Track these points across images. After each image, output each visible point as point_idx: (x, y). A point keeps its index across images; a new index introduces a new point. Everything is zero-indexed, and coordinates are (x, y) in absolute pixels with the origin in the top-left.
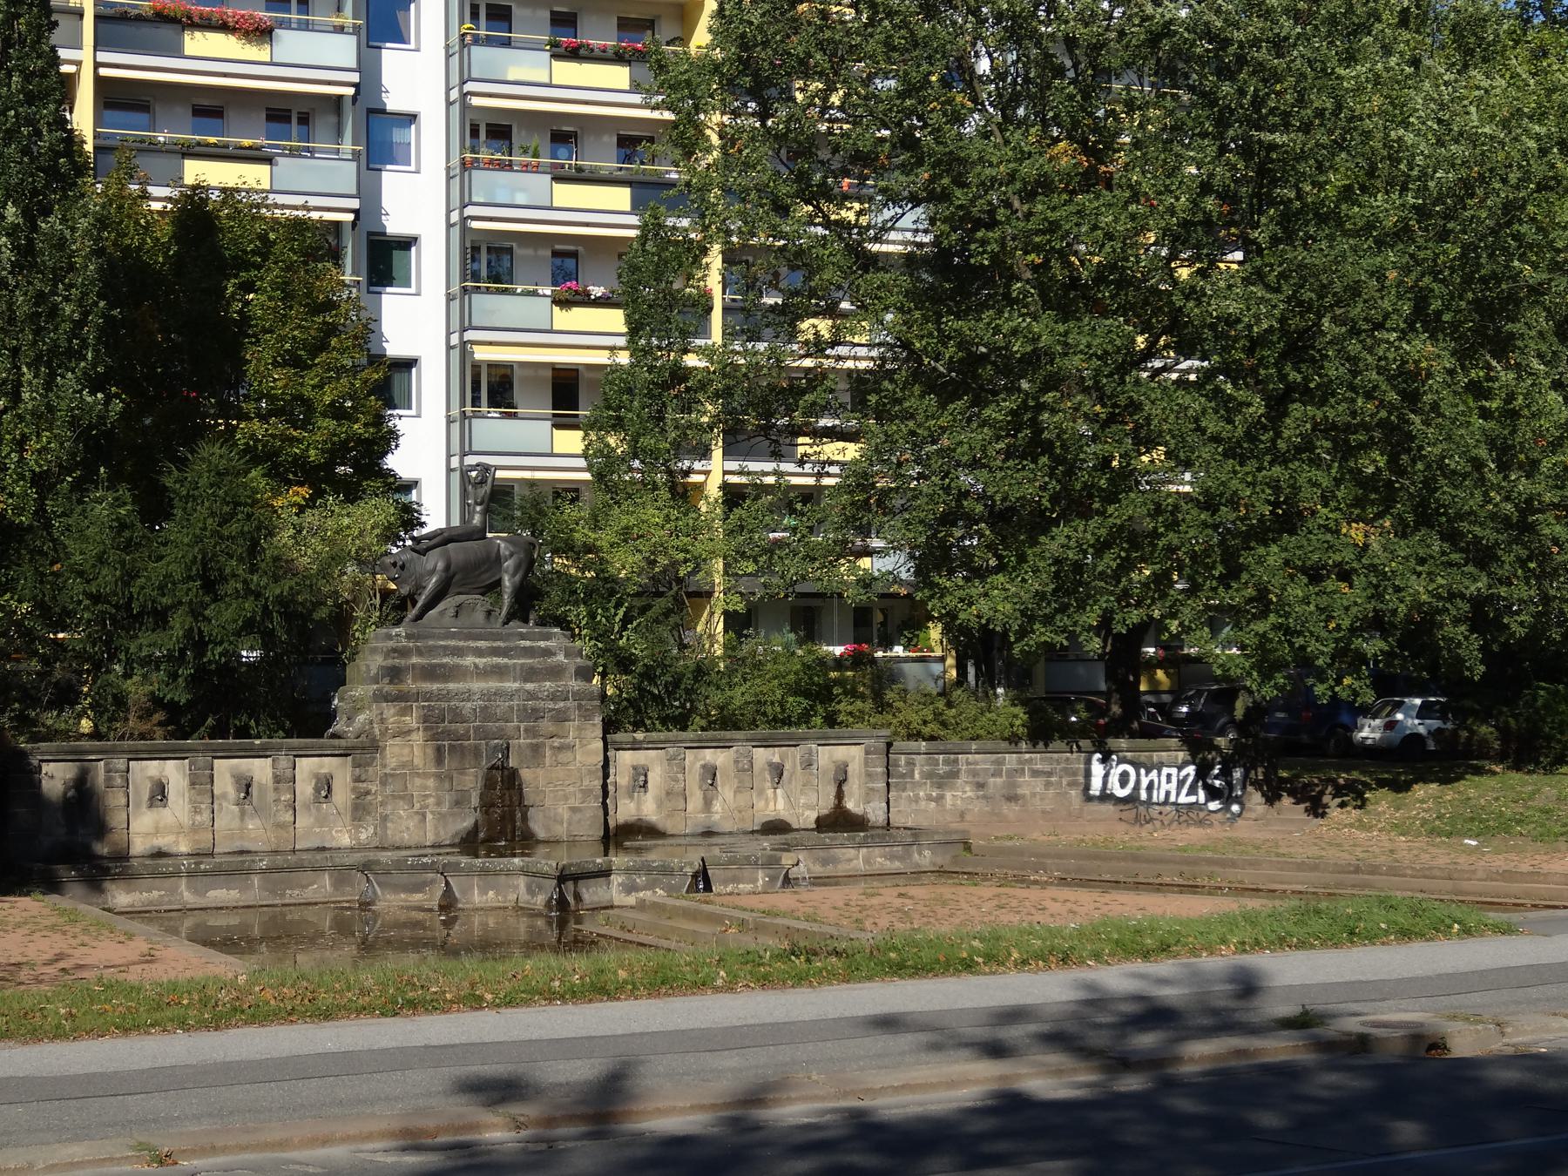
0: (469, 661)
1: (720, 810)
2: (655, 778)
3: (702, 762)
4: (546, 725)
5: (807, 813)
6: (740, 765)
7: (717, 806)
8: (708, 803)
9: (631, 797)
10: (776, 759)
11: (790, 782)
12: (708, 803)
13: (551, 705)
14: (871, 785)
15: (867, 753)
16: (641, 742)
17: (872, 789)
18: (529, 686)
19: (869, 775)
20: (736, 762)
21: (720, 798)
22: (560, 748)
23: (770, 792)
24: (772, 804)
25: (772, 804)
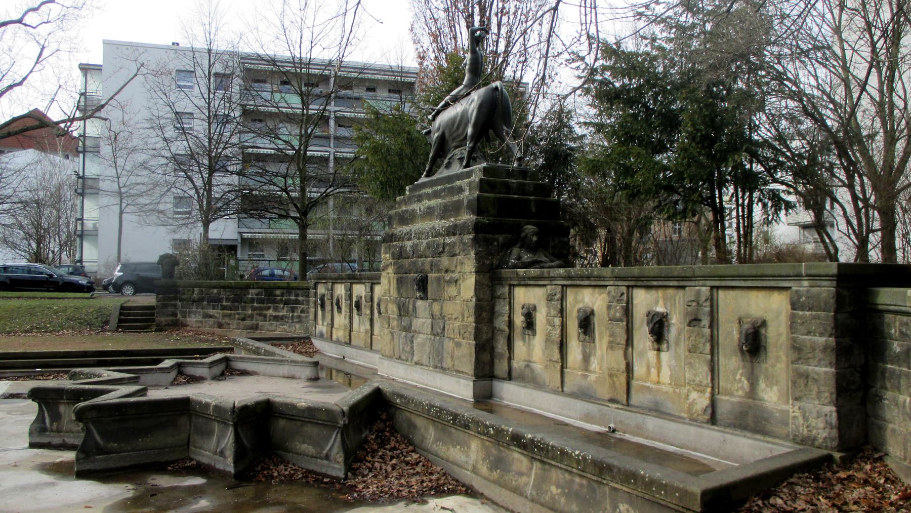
0: (416, 207)
1: (597, 370)
2: (540, 318)
3: (581, 305)
4: (445, 261)
5: (694, 395)
6: (612, 312)
7: (594, 365)
8: (586, 359)
9: (524, 339)
10: (660, 309)
11: (677, 343)
12: (586, 359)
13: (448, 240)
14: (803, 367)
15: (794, 305)
16: (523, 278)
17: (806, 376)
18: (438, 224)
19: (796, 348)
20: (609, 307)
21: (598, 352)
22: (449, 282)
23: (652, 354)
24: (653, 371)
25: (653, 371)
